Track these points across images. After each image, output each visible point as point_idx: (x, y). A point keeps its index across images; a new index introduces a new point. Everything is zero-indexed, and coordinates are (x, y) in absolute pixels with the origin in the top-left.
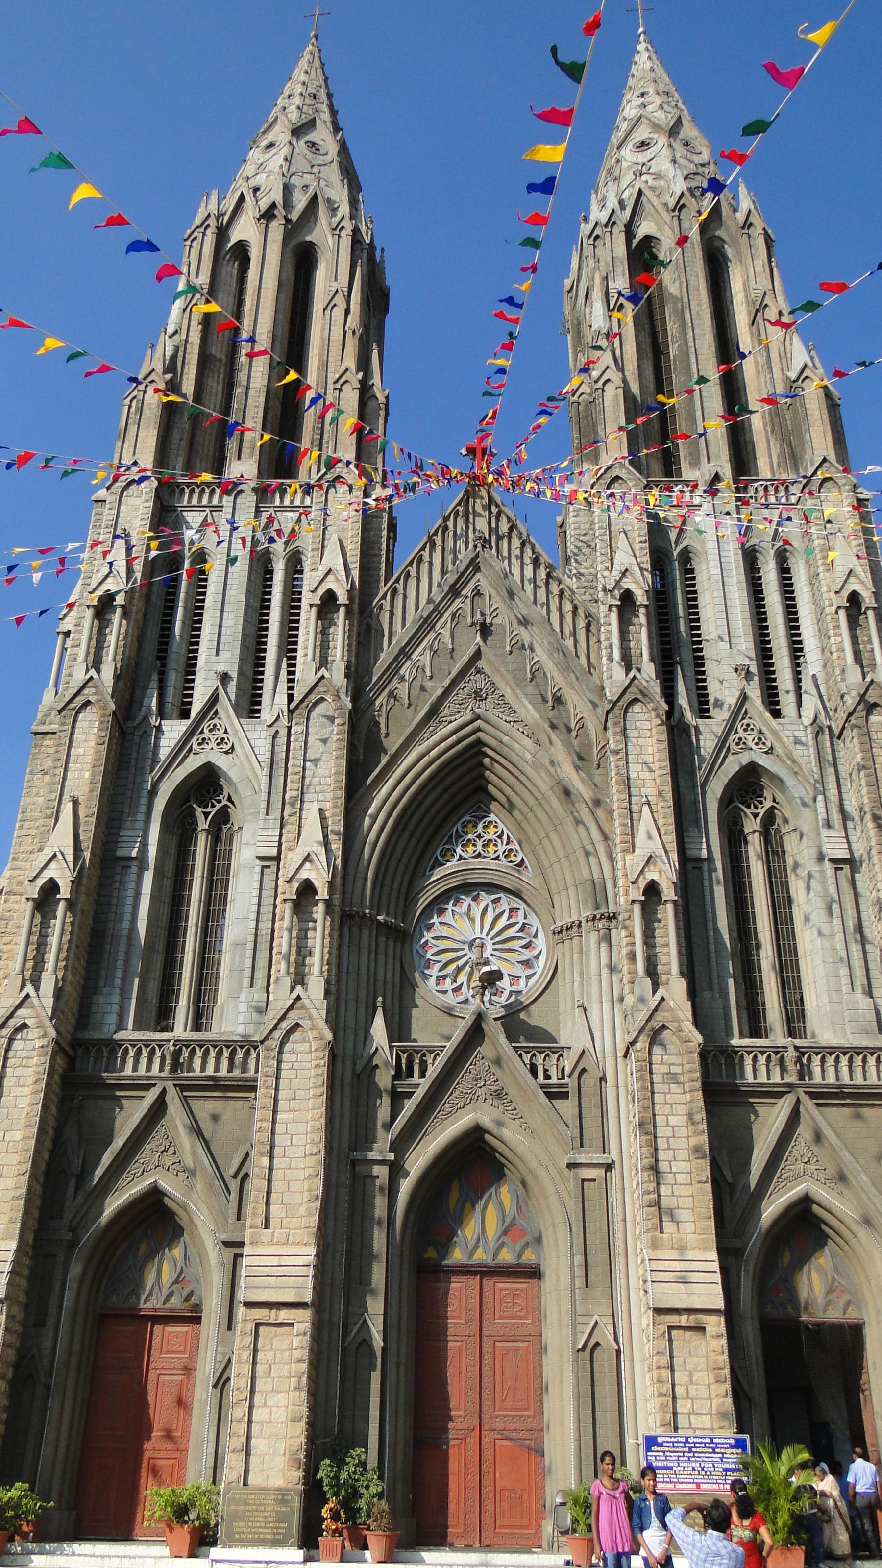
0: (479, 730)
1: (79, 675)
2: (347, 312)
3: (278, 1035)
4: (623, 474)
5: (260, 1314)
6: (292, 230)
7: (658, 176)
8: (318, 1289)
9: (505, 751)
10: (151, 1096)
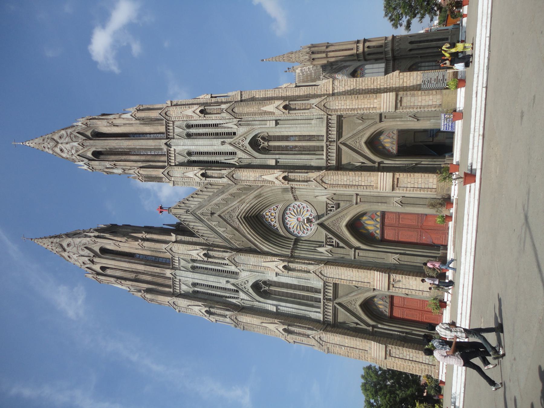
0: (241, 217)
1: (228, 320)
2: (121, 242)
3: (322, 277)
4: (166, 172)
5: (391, 286)
6: (96, 255)
7: (72, 148)
8: (385, 273)
9: (246, 211)
10: (337, 306)
